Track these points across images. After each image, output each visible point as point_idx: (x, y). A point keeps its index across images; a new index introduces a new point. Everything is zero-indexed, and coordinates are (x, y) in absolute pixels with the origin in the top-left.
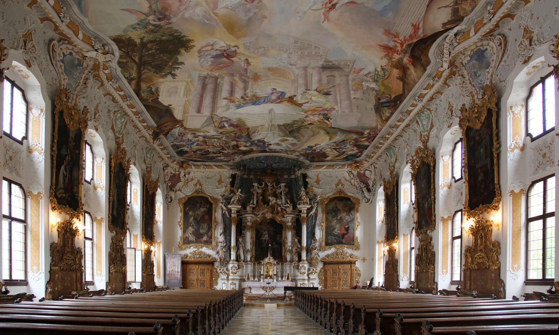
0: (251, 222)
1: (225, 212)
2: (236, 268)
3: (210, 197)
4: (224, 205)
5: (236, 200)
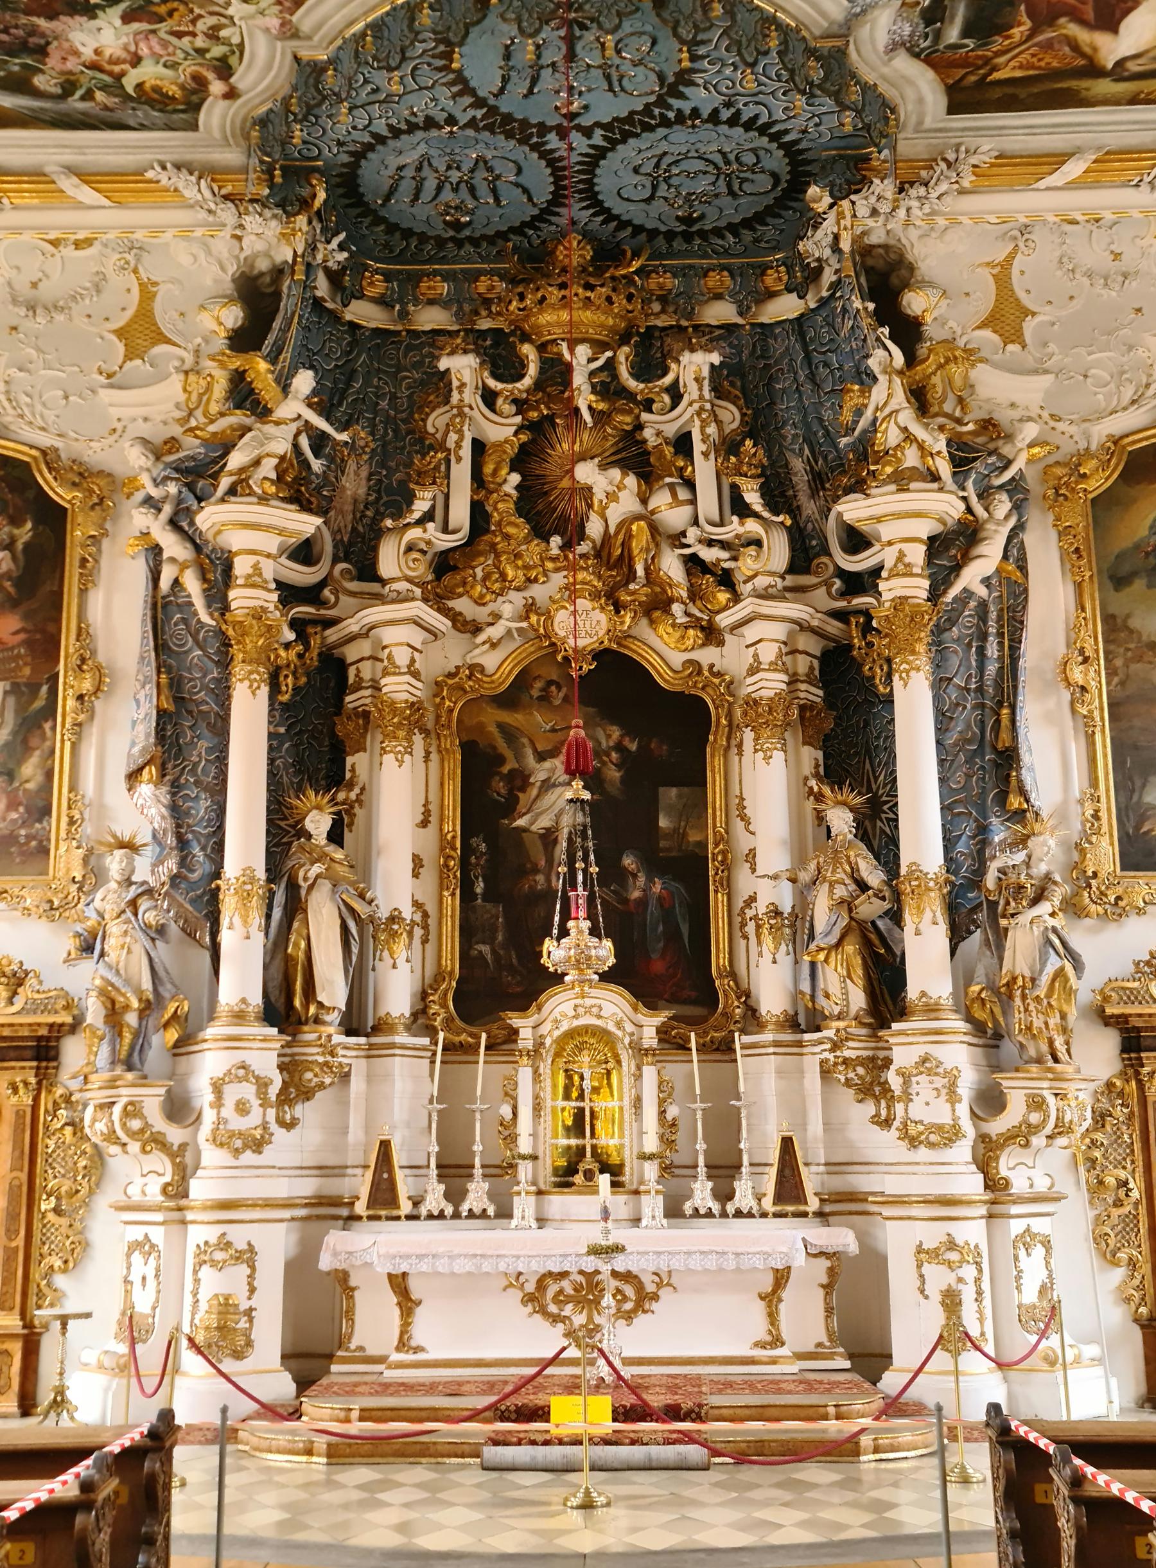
0: (416, 675)
1: (176, 582)
2: (262, 1085)
3: (49, 456)
4: (173, 523)
5: (268, 468)
